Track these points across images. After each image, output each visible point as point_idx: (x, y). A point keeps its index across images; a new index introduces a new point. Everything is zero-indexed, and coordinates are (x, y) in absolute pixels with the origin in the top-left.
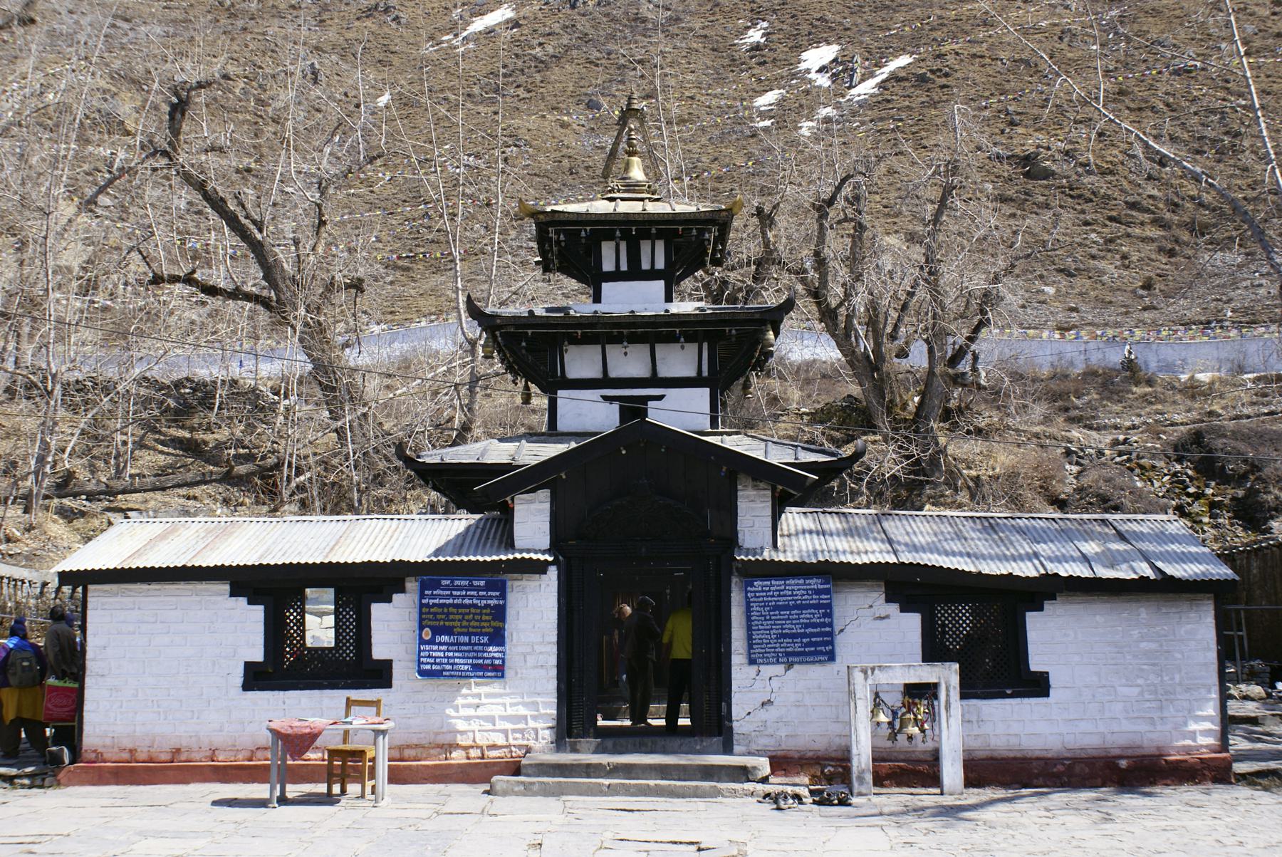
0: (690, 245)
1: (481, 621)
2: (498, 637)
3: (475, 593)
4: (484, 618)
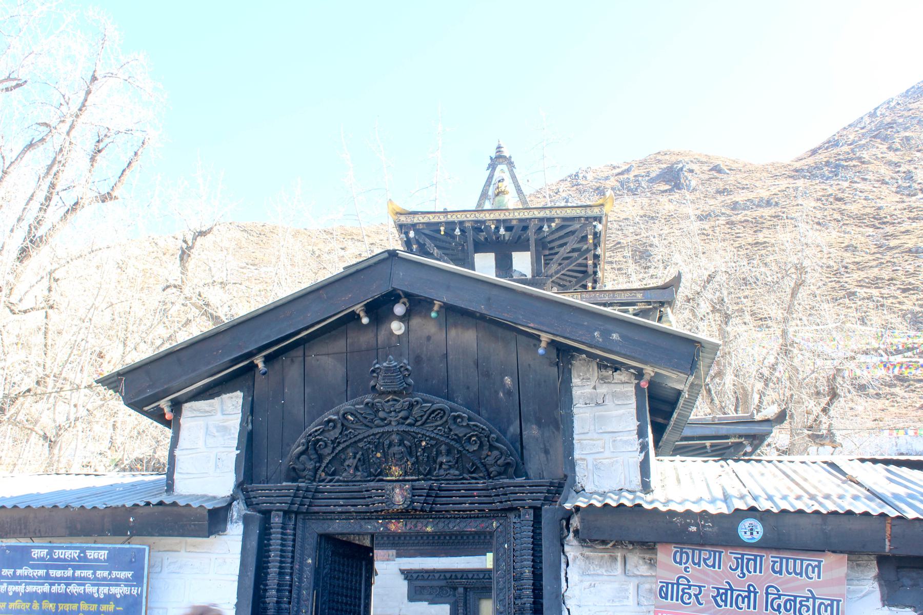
3: (88, 573)
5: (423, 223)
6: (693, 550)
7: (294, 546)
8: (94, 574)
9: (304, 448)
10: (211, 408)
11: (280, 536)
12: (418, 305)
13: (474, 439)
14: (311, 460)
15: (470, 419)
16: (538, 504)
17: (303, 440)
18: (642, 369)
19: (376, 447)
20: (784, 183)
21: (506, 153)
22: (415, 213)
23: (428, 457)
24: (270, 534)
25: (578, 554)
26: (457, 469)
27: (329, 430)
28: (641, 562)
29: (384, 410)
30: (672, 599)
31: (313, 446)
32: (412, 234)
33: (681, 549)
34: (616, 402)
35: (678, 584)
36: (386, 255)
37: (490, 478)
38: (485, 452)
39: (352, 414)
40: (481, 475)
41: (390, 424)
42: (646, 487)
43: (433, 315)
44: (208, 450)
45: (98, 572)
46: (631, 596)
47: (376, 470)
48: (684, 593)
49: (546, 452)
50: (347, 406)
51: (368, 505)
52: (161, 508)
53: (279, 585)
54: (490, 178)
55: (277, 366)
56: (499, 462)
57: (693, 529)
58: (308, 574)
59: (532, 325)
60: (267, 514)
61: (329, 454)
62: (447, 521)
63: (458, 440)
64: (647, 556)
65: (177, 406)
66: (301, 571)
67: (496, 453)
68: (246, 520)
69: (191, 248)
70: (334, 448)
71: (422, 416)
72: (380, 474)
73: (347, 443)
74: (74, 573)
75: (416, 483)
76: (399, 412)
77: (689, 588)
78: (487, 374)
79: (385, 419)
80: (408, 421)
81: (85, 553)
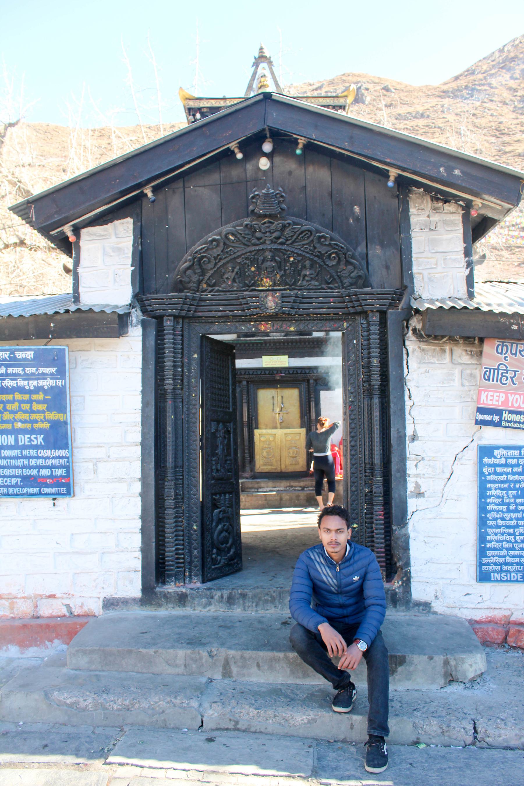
1: (32, 412)
2: (58, 436)
3: (18, 370)
4: (36, 407)
5: (207, 108)
6: (512, 344)
7: (182, 344)
8: (24, 370)
9: (191, 263)
10: (106, 233)
11: (172, 336)
12: (283, 142)
13: (334, 255)
14: (195, 273)
15: (332, 239)
16: (384, 308)
17: (190, 257)
18: (472, 201)
19: (251, 262)
20: (434, 101)
21: (267, 54)
22: (201, 99)
23: (294, 271)
24: (164, 335)
25: (416, 347)
26: (317, 281)
27: (213, 248)
28: (464, 353)
29: (260, 231)
30: (493, 381)
31: (198, 263)
33: (503, 343)
34: (446, 228)
35: (498, 369)
36: (261, 97)
37: (343, 288)
38: (342, 266)
39: (233, 235)
40: (336, 285)
41: (264, 243)
42: (471, 295)
43: (298, 152)
45: (27, 369)
46: (456, 379)
47: (250, 282)
48: (502, 376)
49: (387, 267)
50: (228, 228)
51: (244, 310)
52: (77, 315)
53: (174, 375)
54: (255, 73)
55: (161, 196)
56: (352, 275)
57: (515, 327)
58: (195, 367)
59: (388, 160)
60: (160, 319)
61: (212, 269)
62: (307, 323)
63: (320, 256)
64: (469, 349)
65: (76, 230)
66: (190, 364)
67: (350, 267)
68: (144, 324)
70: (216, 264)
71: (292, 236)
72: (253, 285)
73: (227, 259)
74: (6, 371)
75: (284, 292)
76: (273, 233)
77: (507, 373)
78: (340, 204)
79: (261, 238)
80: (280, 240)
81: (14, 354)
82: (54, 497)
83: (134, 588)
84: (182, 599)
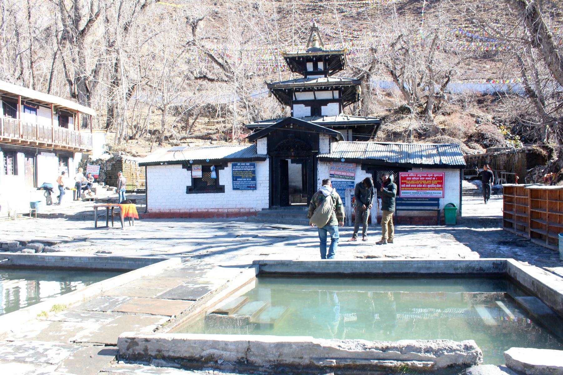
0: (334, 62)
2: (254, 179)
32: (288, 60)
42: (330, 153)
44: (262, 147)
60: (272, 157)
69: (196, 26)
82: (253, 190)
83: (267, 207)
84: (276, 209)
